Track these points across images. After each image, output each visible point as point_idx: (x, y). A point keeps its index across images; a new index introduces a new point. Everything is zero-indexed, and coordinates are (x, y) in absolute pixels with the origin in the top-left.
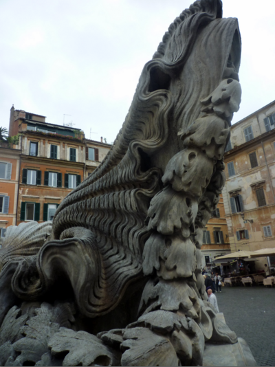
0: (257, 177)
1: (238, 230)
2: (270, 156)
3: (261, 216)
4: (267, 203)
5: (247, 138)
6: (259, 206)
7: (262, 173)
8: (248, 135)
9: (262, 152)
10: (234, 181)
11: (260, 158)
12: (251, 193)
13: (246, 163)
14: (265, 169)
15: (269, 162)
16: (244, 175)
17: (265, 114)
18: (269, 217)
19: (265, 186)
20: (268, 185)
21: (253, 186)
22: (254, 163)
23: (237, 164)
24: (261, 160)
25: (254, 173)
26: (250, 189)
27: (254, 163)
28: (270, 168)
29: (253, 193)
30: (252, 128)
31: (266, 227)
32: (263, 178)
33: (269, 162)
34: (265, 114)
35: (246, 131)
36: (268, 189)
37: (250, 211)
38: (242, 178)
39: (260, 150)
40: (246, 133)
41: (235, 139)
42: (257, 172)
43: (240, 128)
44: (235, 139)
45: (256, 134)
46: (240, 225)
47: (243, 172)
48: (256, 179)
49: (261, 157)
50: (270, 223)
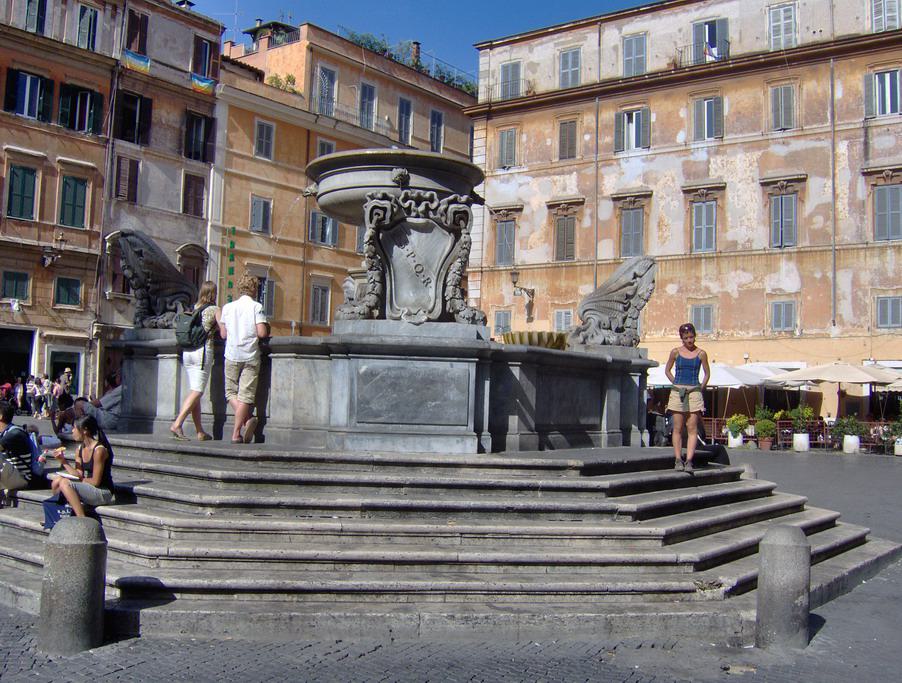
0: (568, 186)
3: (557, 283)
4: (578, 256)
5: (564, 77)
6: (557, 259)
8: (570, 70)
9: (594, 125)
10: (508, 181)
11: (584, 139)
12: (544, 221)
14: (590, 171)
16: (536, 173)
17: (620, 30)
18: (575, 290)
19: (582, 214)
20: (587, 211)
21: (550, 207)
22: (567, 149)
23: (524, 138)
24: (586, 146)
25: (563, 173)
26: (546, 211)
27: (567, 149)
28: (602, 171)
29: (550, 223)
30: (582, 56)
31: (563, 311)
32: (582, 191)
33: (601, 155)
34: (620, 30)
35: (564, 57)
36: (587, 222)
37: (530, 268)
38: (530, 179)
39: (588, 119)
40: (565, 64)
41: (534, 72)
42: (570, 173)
43: (551, 44)
44: (534, 72)
45: (589, 76)
46: (502, 298)
47: (537, 164)
48: (564, 189)
49: (587, 137)
50: (574, 304)
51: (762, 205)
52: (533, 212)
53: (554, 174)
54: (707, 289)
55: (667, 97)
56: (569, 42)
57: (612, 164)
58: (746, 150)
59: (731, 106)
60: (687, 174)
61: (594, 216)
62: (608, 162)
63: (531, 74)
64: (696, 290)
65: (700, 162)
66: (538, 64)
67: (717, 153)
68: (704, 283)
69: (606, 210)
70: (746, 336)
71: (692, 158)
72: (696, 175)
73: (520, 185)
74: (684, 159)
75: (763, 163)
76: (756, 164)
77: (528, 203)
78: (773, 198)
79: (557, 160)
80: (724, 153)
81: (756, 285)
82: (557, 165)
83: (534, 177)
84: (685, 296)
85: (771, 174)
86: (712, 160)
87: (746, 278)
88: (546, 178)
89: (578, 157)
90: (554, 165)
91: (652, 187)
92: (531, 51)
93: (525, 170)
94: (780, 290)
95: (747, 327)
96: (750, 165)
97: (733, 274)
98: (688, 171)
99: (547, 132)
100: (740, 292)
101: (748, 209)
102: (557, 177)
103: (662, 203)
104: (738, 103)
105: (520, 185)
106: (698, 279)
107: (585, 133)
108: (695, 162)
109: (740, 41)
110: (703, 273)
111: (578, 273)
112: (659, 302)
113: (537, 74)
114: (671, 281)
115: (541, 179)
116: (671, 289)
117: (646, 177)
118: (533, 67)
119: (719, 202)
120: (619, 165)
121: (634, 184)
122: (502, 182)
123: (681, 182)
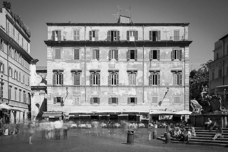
0: (77, 66)
1: (55, 97)
2: (88, 56)
3: (75, 90)
7: (81, 65)
10: (59, 63)
11: (81, 55)
13: (71, 54)
14: (84, 63)
15: (86, 59)
16: (68, 62)
17: (91, 28)
18: (80, 93)
22: (77, 57)
23: (63, 52)
25: (76, 63)
27: (77, 57)
28: (87, 63)
34: (91, 28)
38: (66, 63)
40: (75, 34)
42: (78, 63)
46: (58, 93)
48: (76, 67)
49: (82, 54)
51: (128, 76)
52: (67, 72)
53: (73, 63)
54: (115, 94)
55: (104, 48)
56: (76, 28)
57: (90, 62)
58: (124, 63)
59: (120, 52)
60: (110, 67)
61: (85, 74)
62: (88, 61)
63: (65, 35)
64: (112, 94)
65: (113, 64)
66: (67, 33)
67: (117, 63)
68: (114, 92)
69: (88, 74)
70: (124, 105)
71: (110, 63)
72: (112, 67)
73: (63, 64)
74: (108, 63)
75: (128, 66)
76: (126, 66)
77: (65, 70)
78: (130, 74)
79: (74, 59)
80: (119, 63)
81: (126, 93)
82: (74, 60)
83: (67, 63)
84: (109, 95)
85: (130, 69)
86: (116, 64)
87: (124, 92)
88: (71, 63)
89: (80, 59)
90: (72, 60)
91: (100, 69)
92: (64, 28)
93: (65, 60)
94: (132, 94)
95: (124, 102)
96: (125, 66)
97: (121, 90)
98: (110, 66)
99: (70, 51)
100: (123, 95)
101: (124, 76)
102: (74, 64)
103: (103, 73)
104: (122, 52)
105: (63, 64)
106: (112, 91)
107: (82, 53)
108: (111, 64)
109: (122, 37)
110: (114, 90)
111: (81, 88)
112: (103, 96)
113: (67, 35)
114: (106, 91)
115: (69, 64)
116: (106, 93)
117: (99, 67)
118: (65, 33)
119: (118, 74)
120: (92, 63)
121: (95, 68)
122: (57, 63)
123: (108, 69)
